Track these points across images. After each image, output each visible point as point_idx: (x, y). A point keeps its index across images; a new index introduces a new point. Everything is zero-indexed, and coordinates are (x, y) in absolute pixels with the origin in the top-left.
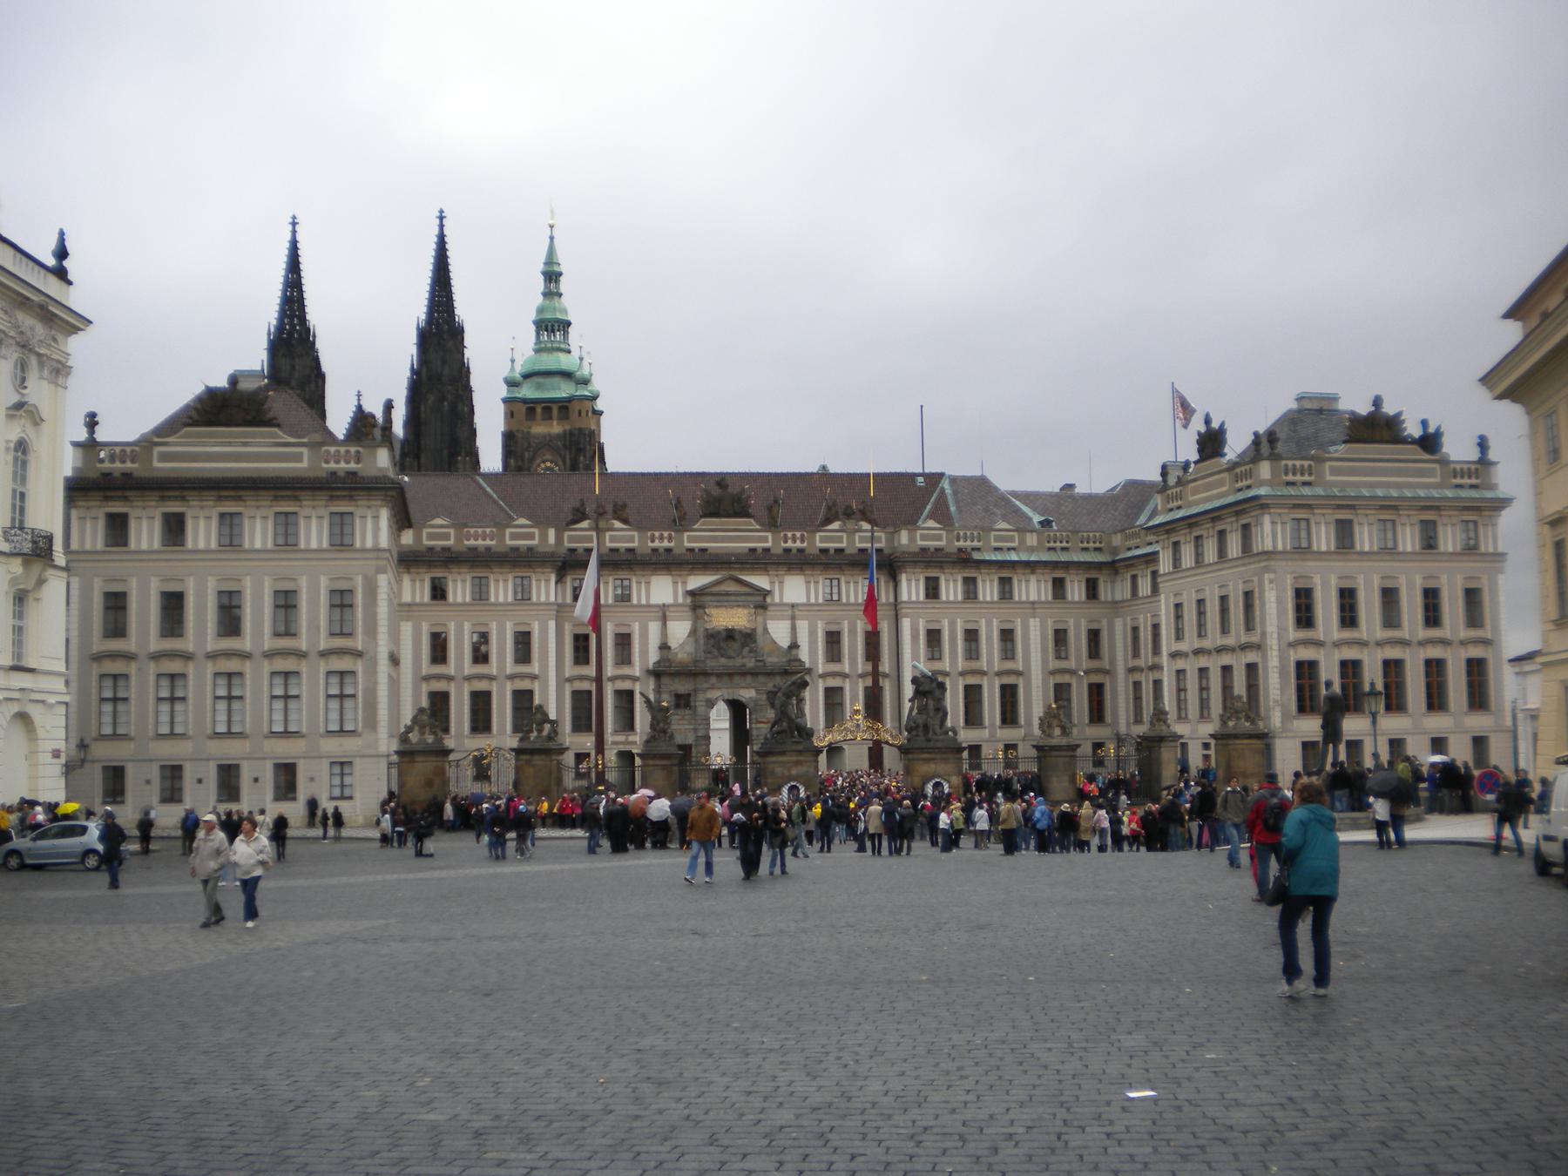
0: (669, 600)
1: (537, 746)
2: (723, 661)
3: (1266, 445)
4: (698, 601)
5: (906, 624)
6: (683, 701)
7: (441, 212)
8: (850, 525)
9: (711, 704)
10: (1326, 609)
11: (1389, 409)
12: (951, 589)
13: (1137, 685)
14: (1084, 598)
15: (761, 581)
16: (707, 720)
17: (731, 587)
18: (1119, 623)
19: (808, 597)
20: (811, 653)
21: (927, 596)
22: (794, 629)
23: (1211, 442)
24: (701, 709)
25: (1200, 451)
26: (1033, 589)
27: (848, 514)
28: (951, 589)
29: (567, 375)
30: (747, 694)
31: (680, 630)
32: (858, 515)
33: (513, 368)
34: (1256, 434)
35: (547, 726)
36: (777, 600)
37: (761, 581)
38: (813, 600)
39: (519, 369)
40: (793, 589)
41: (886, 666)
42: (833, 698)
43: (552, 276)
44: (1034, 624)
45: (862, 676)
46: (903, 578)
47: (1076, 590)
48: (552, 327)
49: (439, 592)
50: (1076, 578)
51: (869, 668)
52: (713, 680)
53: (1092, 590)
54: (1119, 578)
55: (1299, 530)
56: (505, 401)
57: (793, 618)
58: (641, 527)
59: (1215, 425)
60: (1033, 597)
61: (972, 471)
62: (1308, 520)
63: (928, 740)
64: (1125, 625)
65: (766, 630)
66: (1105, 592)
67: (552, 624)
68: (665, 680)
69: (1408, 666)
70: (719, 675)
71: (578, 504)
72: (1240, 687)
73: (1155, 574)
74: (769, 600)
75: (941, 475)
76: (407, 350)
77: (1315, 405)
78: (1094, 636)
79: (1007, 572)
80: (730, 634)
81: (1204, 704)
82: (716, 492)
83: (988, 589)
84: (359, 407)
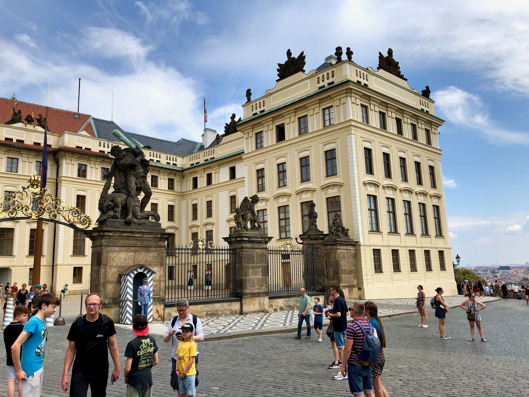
8: (30, 127)
14: (167, 189)
21: (79, 175)
27: (29, 120)
32: (36, 121)
53: (171, 187)
59: (295, 55)
73: (209, 176)
75: (89, 116)
78: (171, 209)
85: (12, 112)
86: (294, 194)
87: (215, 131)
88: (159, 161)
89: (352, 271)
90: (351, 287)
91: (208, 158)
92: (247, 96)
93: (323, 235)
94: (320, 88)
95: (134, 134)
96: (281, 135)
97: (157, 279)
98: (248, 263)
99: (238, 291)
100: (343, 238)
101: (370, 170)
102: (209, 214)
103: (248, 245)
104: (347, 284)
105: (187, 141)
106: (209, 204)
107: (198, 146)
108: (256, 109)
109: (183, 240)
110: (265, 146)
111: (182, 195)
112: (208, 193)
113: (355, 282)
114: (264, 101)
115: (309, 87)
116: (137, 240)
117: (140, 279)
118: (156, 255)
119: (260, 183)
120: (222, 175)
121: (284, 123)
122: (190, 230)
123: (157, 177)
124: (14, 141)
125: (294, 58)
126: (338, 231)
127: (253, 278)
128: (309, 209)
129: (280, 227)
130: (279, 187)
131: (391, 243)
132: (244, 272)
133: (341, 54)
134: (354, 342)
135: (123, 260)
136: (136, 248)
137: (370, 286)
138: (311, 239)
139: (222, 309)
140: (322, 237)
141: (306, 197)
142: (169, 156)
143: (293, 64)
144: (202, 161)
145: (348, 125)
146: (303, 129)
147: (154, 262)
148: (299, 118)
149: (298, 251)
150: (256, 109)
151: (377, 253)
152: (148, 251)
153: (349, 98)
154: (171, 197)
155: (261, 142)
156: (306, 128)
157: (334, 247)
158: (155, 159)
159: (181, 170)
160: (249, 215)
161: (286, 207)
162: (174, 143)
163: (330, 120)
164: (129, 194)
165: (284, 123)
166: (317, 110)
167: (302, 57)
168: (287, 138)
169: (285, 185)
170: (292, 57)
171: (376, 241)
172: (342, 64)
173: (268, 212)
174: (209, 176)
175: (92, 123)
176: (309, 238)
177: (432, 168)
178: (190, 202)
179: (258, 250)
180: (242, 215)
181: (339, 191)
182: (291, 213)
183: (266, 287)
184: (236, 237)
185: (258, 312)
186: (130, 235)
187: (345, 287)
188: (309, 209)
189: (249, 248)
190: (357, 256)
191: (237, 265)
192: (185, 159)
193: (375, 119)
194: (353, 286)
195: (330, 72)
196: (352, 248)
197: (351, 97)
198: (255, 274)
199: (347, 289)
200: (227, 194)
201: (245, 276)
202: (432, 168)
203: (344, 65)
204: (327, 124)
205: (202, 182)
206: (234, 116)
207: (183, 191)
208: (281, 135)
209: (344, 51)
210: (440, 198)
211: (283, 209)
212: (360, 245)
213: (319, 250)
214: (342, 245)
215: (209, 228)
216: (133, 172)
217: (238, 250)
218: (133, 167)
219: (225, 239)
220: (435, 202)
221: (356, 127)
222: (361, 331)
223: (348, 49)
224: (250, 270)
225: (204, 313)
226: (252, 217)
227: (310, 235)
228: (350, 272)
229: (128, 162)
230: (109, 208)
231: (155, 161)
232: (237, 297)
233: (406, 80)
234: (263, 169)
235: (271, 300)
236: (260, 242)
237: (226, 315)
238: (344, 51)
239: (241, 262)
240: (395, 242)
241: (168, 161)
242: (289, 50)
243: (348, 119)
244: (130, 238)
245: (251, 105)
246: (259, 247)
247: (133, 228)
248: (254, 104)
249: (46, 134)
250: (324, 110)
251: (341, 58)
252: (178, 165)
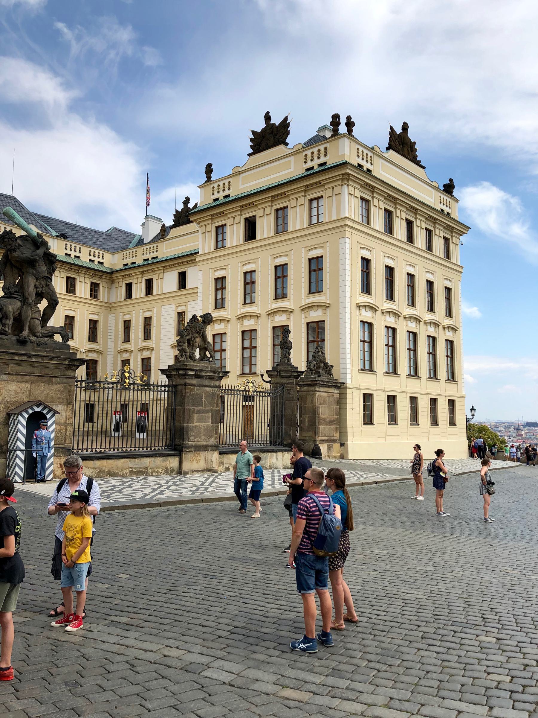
11: (412, 135)
14: (88, 296)
54: (115, 285)
59: (276, 120)
63: (23, 342)
73: (149, 283)
78: (93, 324)
86: (264, 314)
87: (160, 220)
88: (79, 257)
89: (333, 421)
90: (330, 442)
91: (149, 256)
92: (206, 173)
93: (298, 372)
94: (307, 170)
95: (44, 217)
96: (251, 231)
97: (62, 422)
98: (193, 405)
99: (177, 443)
100: (324, 378)
101: (367, 288)
102: (147, 336)
103: (195, 381)
104: (326, 438)
105: (120, 231)
106: (148, 321)
107: (136, 240)
108: (218, 192)
109: (108, 371)
110: (228, 245)
111: (110, 307)
112: (147, 306)
113: (337, 436)
114: (229, 182)
115: (294, 168)
116: (34, 366)
117: (36, 421)
118: (62, 389)
119: (219, 297)
120: (168, 282)
121: (256, 216)
122: (119, 355)
123: (75, 279)
125: (274, 124)
126: (319, 367)
127: (199, 424)
128: (282, 334)
129: (243, 358)
130: (245, 303)
131: (388, 387)
132: (186, 418)
133: (339, 124)
134: (307, 523)
135: (13, 393)
136: (32, 378)
137: (356, 442)
138: (282, 377)
139: (153, 466)
140: (296, 374)
141: (280, 320)
142: (93, 250)
143: (272, 132)
144: (139, 262)
145: (341, 225)
146: (281, 226)
147: (59, 398)
148: (277, 210)
149: (262, 392)
150: (218, 192)
151: (368, 398)
152: (50, 383)
153: (346, 186)
154: (94, 309)
155: (223, 240)
156: (285, 224)
157: (312, 388)
158: (73, 254)
159: (109, 271)
160: (198, 340)
161: (253, 333)
162: (101, 233)
163: (318, 215)
164: (24, 301)
165: (256, 216)
166: (301, 201)
167: (285, 124)
168: (258, 237)
169: (252, 302)
170: (272, 122)
172: (339, 138)
173: (228, 338)
174: (149, 283)
176: (279, 375)
177: (448, 290)
178: (120, 317)
179: (208, 389)
180: (189, 340)
181: (324, 314)
182: (259, 340)
183: (216, 438)
184: (178, 370)
185: (203, 471)
186: (25, 358)
187: (322, 441)
188: (282, 334)
189: (195, 386)
190: (341, 401)
191: (178, 408)
192: (116, 256)
193: (378, 219)
194: (334, 441)
195: (322, 148)
196: (336, 391)
197: (348, 185)
198: (200, 420)
199: (326, 445)
200: (174, 309)
201: (188, 422)
202: (448, 290)
203: (341, 140)
204: (314, 221)
205: (139, 290)
206: (187, 200)
207: (110, 302)
208: (251, 231)
209: (343, 121)
210: (456, 330)
211: (248, 335)
212: (346, 388)
213: (291, 392)
214: (322, 386)
215: (146, 354)
216: (31, 270)
217: (179, 388)
218: (32, 263)
219: (163, 371)
220: (449, 335)
221: (352, 228)
222: (317, 508)
223: (349, 118)
224: (195, 415)
225: (128, 471)
226: (202, 344)
227: (281, 371)
228: (331, 422)
229: (24, 255)
231: (73, 256)
232: (175, 449)
233: (423, 168)
234: (225, 277)
235: (221, 456)
236: (211, 378)
237: (159, 474)
238: (343, 121)
239: (182, 404)
240: (392, 385)
241: (92, 258)
242: (268, 113)
243: (342, 217)
244: (25, 363)
245: (212, 186)
246: (209, 384)
247: (29, 349)
248: (215, 186)
250: (311, 201)
251: (338, 130)
252: (105, 265)
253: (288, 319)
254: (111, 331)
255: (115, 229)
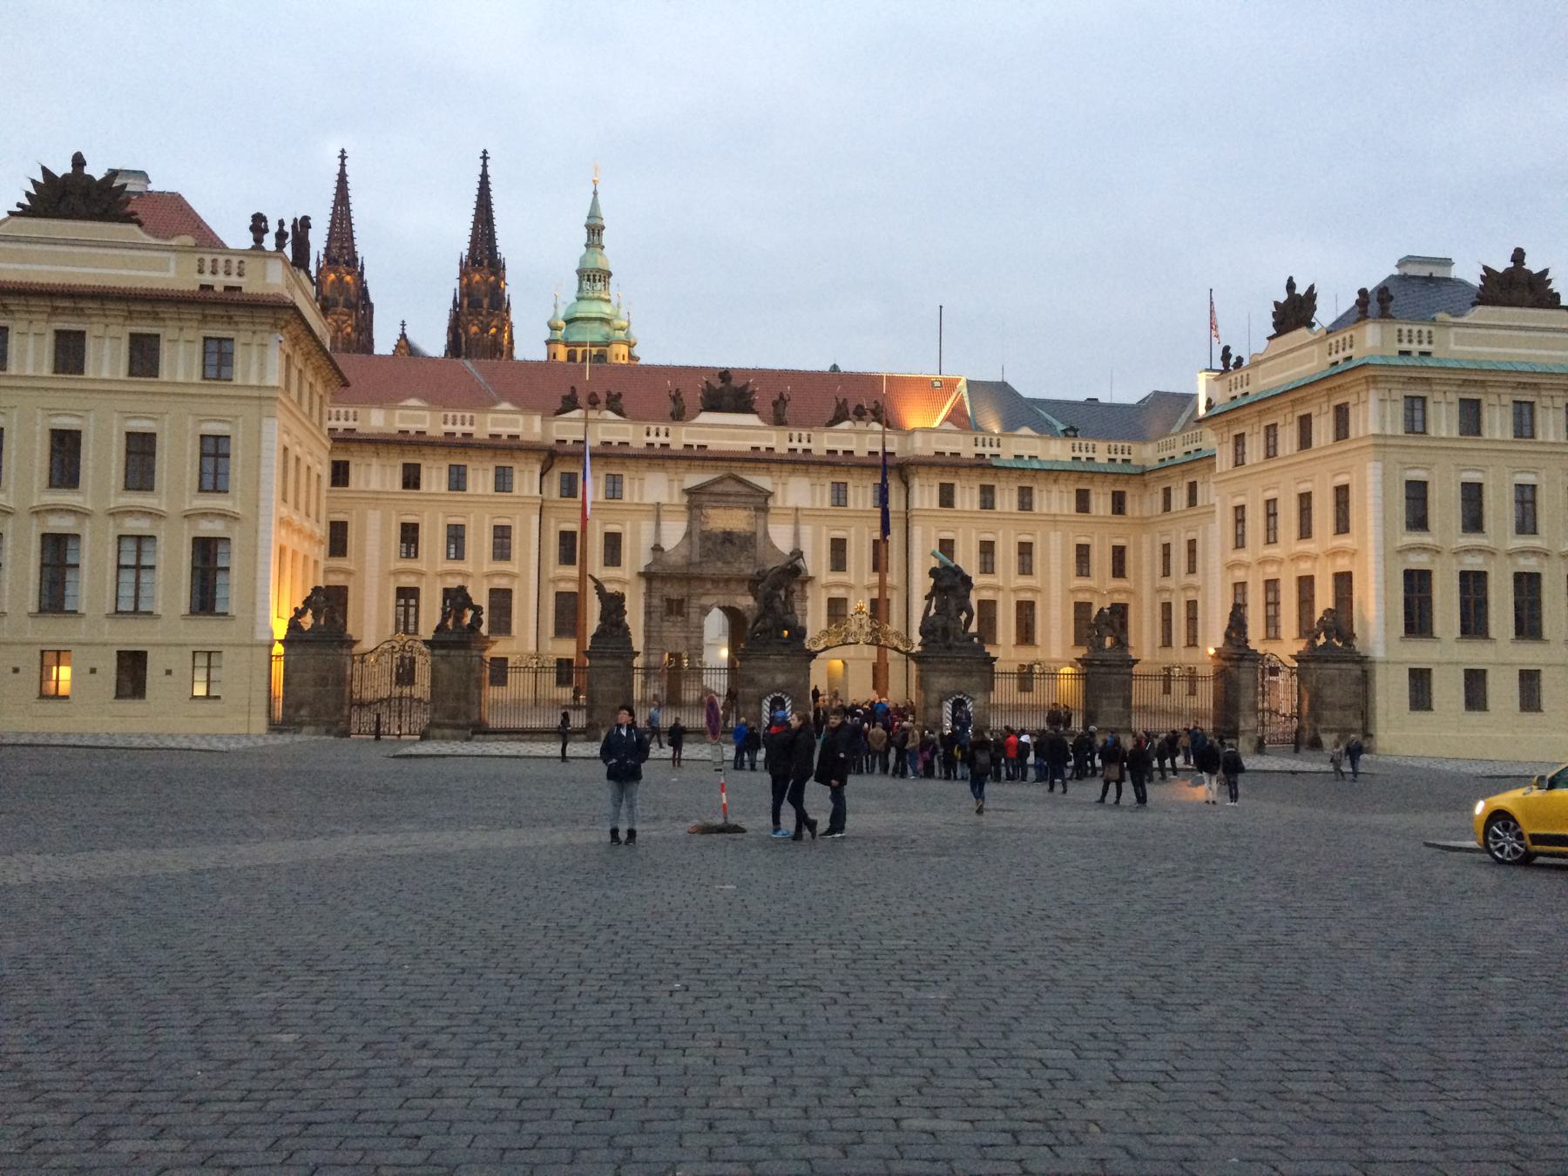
0: (664, 499)
1: (454, 638)
2: (719, 564)
3: (1375, 304)
4: (695, 497)
5: (917, 532)
6: (675, 608)
7: (485, 152)
8: (861, 425)
9: (705, 611)
10: (1445, 507)
11: (1533, 265)
12: (967, 497)
13: (1167, 607)
15: (763, 481)
16: (701, 627)
17: (732, 487)
18: (1146, 539)
19: (813, 500)
20: (816, 562)
22: (797, 535)
23: (1294, 311)
24: (694, 616)
25: (1275, 325)
26: (1055, 500)
27: (860, 414)
28: (967, 497)
29: (604, 321)
30: (745, 602)
31: (674, 533)
32: (870, 416)
33: (555, 314)
34: (1363, 292)
35: (469, 613)
36: (779, 504)
37: (763, 481)
38: (818, 505)
39: (561, 313)
40: (796, 492)
41: (894, 578)
42: (837, 608)
43: (595, 230)
44: (1055, 539)
45: (869, 588)
46: (916, 483)
47: (1101, 504)
48: (593, 277)
49: (411, 479)
50: (1100, 490)
51: (875, 578)
52: (709, 586)
53: (1119, 504)
55: (1413, 409)
56: (548, 343)
57: (797, 523)
58: (637, 418)
59: (1301, 290)
60: (1055, 509)
61: (993, 376)
62: (1424, 399)
63: (949, 648)
64: (1153, 541)
65: (766, 534)
66: (1131, 506)
67: (536, 519)
68: (656, 584)
69: (1546, 582)
70: (715, 581)
71: (567, 392)
72: (1324, 599)
73: (1192, 487)
74: (771, 503)
76: (449, 285)
77: (1424, 271)
78: (1119, 553)
79: (1029, 476)
80: (728, 537)
81: (1272, 622)
82: (718, 384)
83: (1006, 499)
84: (403, 336)
85: (834, 407)
102: (1192, 570)
103: (1103, 670)
106: (1192, 545)
111: (1144, 523)
113: (1358, 724)
124: (840, 453)
144: (1179, 454)
158: (1084, 455)
167: (1311, 294)
171: (1420, 653)
173: (1250, 588)
175: (965, 391)
205: (1179, 498)
211: (1271, 585)
214: (1327, 661)
215: (1191, 595)
218: (953, 588)
228: (1343, 708)
230: (933, 632)
241: (1113, 456)
242: (1290, 279)
249: (884, 433)
253: (1313, 568)
254: (1143, 559)
255: (1156, 393)
